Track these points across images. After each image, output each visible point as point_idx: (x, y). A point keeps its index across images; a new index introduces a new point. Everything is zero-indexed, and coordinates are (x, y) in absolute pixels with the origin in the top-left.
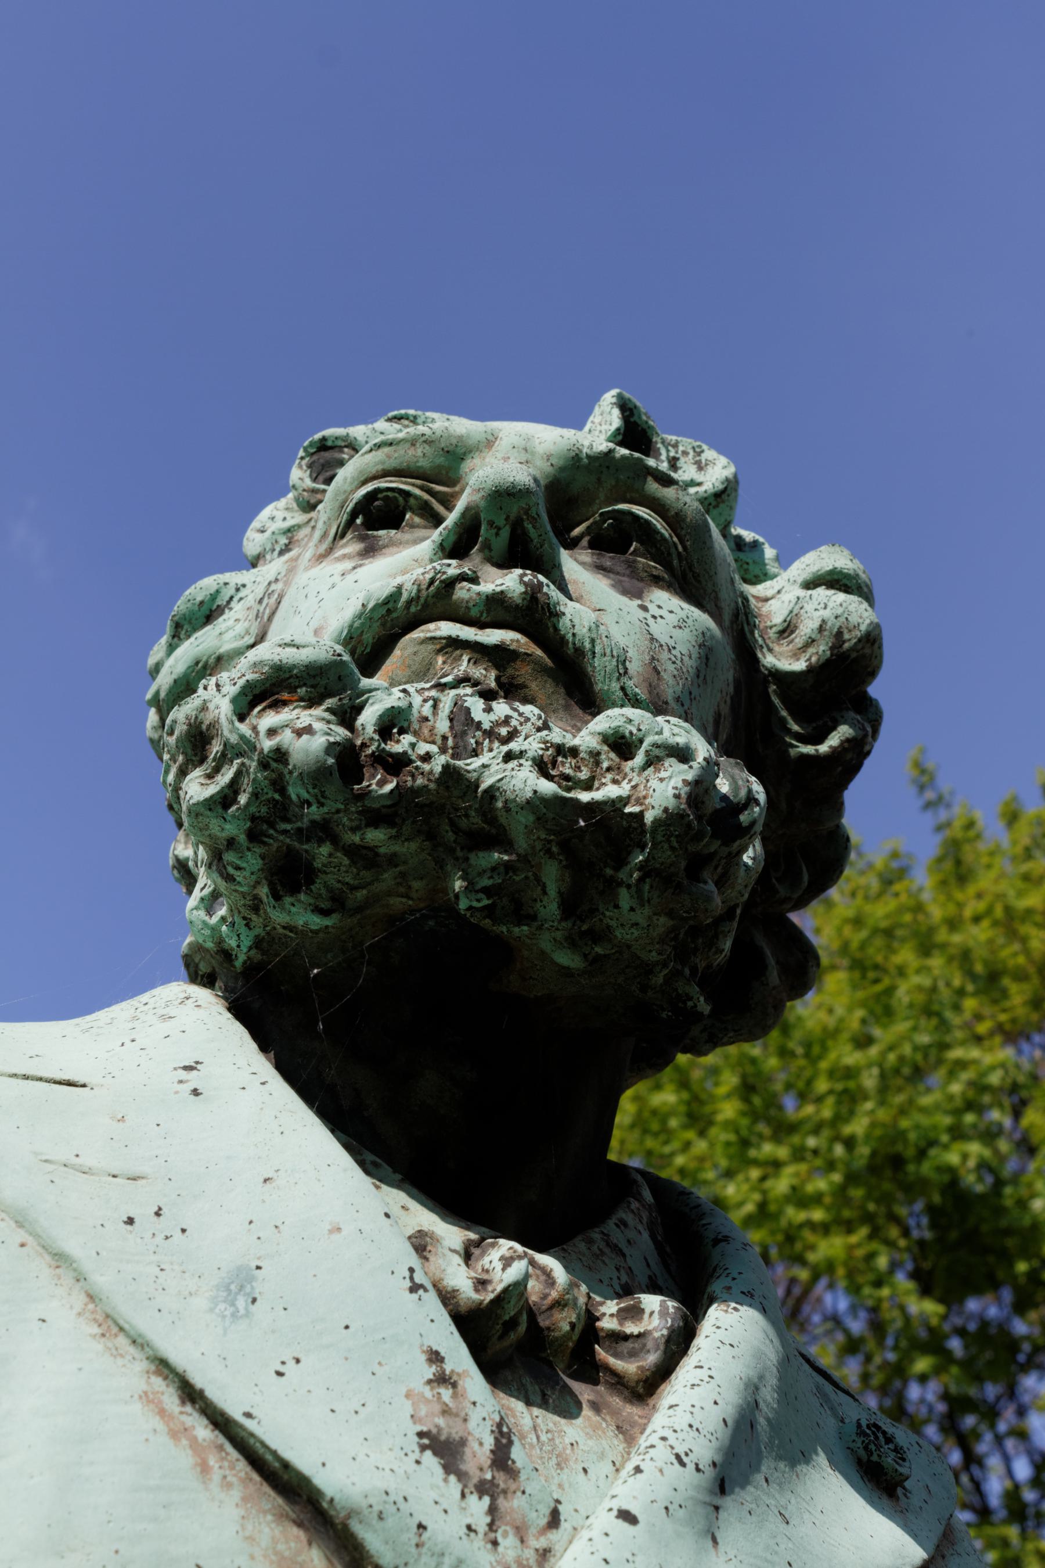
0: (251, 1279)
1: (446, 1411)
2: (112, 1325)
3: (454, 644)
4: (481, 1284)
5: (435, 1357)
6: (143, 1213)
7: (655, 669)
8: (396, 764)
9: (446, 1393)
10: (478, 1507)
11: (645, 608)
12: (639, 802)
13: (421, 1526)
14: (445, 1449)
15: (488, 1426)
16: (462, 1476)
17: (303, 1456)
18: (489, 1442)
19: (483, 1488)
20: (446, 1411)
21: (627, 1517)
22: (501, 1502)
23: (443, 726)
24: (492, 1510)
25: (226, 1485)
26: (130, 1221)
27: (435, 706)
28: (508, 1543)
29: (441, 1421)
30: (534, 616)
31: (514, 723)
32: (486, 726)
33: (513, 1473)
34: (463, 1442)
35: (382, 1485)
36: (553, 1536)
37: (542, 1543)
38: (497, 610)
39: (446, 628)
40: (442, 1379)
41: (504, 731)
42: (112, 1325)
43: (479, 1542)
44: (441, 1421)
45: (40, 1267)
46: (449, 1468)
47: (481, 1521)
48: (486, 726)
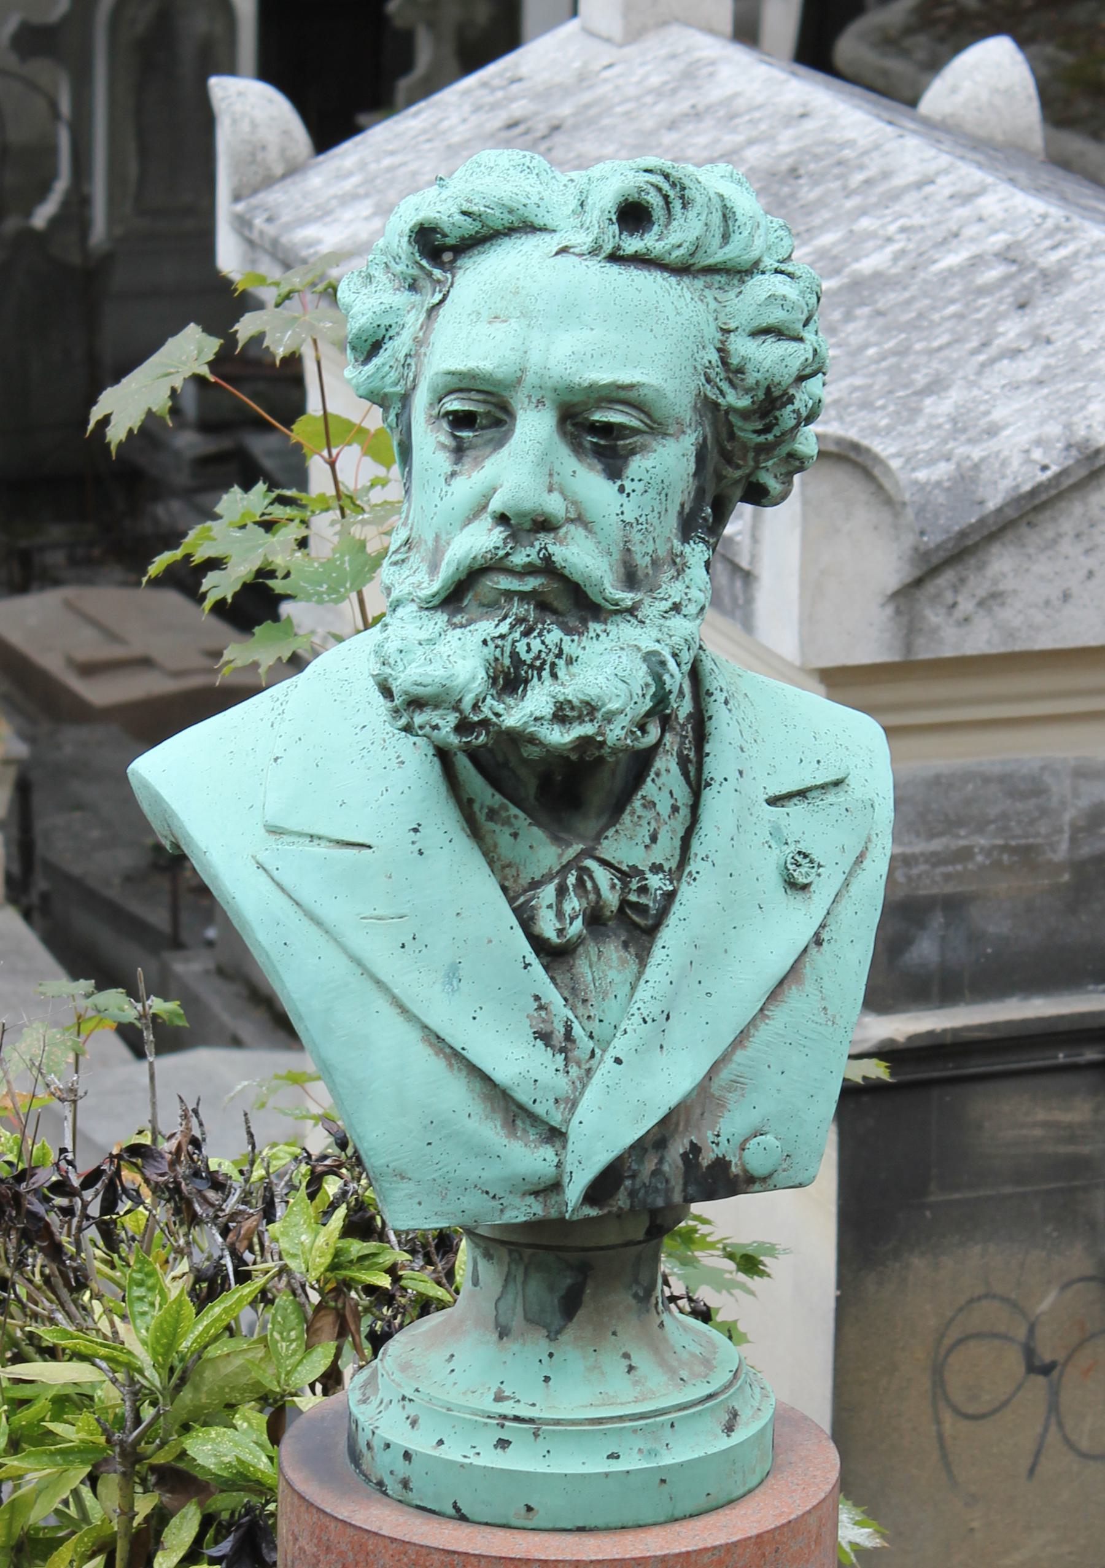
0: (457, 969)
1: (544, 1021)
2: (403, 1010)
3: (509, 594)
4: (560, 932)
5: (537, 998)
6: (407, 939)
7: (629, 550)
8: (485, 723)
9: (543, 1013)
10: (560, 1058)
11: (622, 489)
12: (603, 735)
13: (536, 1081)
14: (544, 1037)
15: (562, 1024)
16: (553, 1047)
17: (487, 1067)
18: (563, 1030)
19: (562, 1050)
20: (544, 1021)
21: (618, 1061)
22: (569, 1054)
23: (507, 662)
24: (566, 1059)
25: (460, 1070)
26: (403, 946)
27: (502, 651)
28: (574, 1071)
29: (542, 1025)
30: (548, 568)
31: (543, 655)
32: (529, 662)
33: (573, 1041)
34: (552, 1032)
35: (518, 1071)
36: (592, 1062)
37: (587, 1066)
38: (529, 570)
39: (506, 583)
40: (541, 1007)
41: (538, 663)
42: (403, 1010)
43: (561, 1074)
44: (542, 1025)
45: (370, 985)
46: (547, 1045)
47: (561, 1066)
48: (529, 662)
